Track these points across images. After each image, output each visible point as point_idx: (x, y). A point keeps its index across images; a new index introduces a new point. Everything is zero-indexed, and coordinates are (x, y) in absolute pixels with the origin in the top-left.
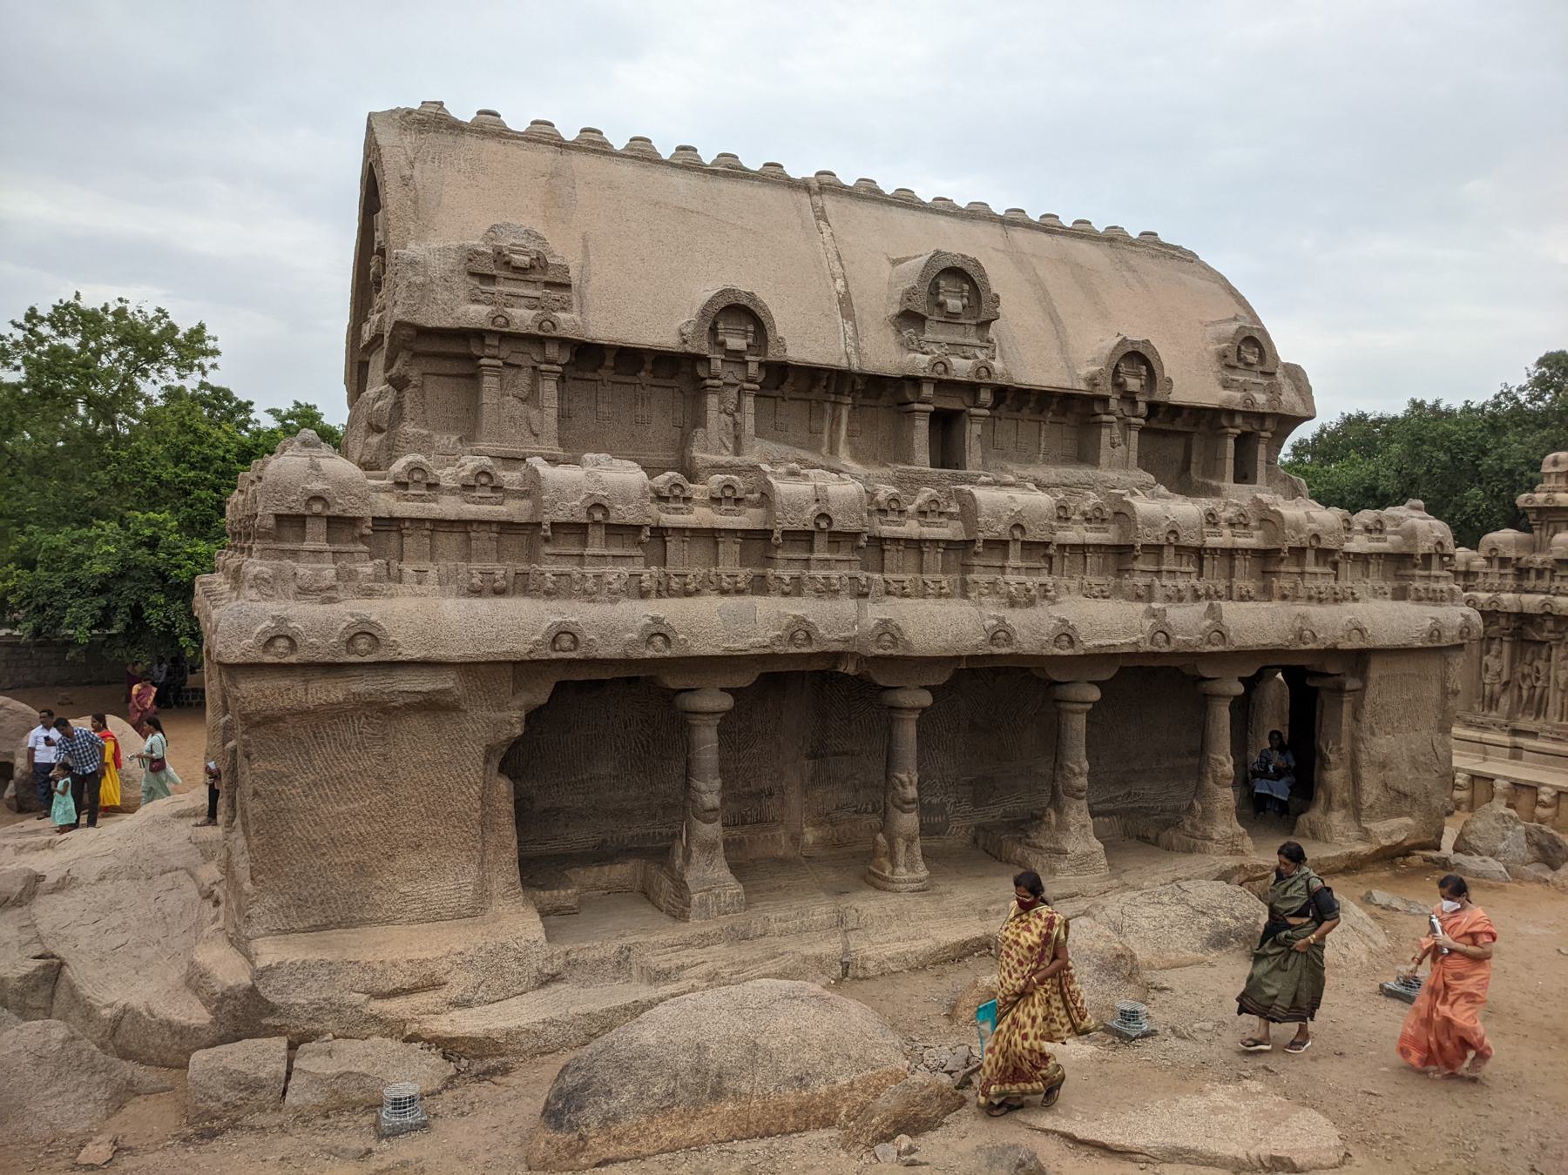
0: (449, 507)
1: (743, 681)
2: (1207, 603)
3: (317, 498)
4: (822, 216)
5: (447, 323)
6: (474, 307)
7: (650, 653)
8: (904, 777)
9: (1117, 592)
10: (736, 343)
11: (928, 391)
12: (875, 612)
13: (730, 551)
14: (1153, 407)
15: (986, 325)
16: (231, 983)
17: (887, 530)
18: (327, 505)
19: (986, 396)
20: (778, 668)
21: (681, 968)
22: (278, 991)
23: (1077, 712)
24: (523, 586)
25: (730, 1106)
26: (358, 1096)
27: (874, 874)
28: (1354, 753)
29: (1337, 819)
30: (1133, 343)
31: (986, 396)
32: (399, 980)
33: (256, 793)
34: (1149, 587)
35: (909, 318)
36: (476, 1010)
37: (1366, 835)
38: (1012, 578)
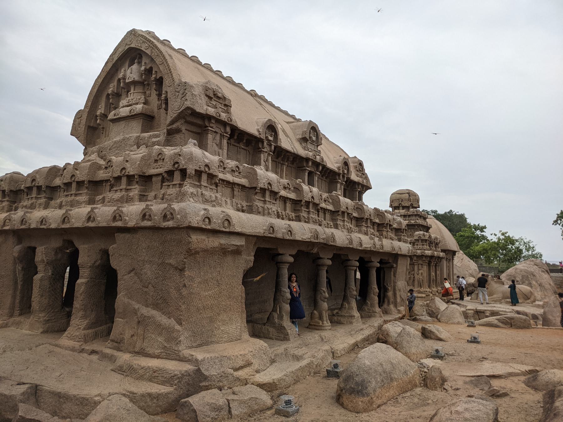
0: (229, 177)
1: (294, 252)
3: (207, 166)
6: (209, 108)
7: (288, 238)
8: (324, 289)
9: (360, 232)
10: (271, 138)
13: (288, 205)
15: (318, 146)
16: (185, 369)
18: (209, 169)
20: (303, 248)
22: (207, 370)
23: (352, 270)
24: (250, 210)
26: (256, 407)
27: (314, 325)
28: (394, 286)
29: (392, 306)
32: (241, 363)
33: (185, 286)
34: (367, 231)
35: (304, 140)
36: (262, 373)
37: (399, 312)
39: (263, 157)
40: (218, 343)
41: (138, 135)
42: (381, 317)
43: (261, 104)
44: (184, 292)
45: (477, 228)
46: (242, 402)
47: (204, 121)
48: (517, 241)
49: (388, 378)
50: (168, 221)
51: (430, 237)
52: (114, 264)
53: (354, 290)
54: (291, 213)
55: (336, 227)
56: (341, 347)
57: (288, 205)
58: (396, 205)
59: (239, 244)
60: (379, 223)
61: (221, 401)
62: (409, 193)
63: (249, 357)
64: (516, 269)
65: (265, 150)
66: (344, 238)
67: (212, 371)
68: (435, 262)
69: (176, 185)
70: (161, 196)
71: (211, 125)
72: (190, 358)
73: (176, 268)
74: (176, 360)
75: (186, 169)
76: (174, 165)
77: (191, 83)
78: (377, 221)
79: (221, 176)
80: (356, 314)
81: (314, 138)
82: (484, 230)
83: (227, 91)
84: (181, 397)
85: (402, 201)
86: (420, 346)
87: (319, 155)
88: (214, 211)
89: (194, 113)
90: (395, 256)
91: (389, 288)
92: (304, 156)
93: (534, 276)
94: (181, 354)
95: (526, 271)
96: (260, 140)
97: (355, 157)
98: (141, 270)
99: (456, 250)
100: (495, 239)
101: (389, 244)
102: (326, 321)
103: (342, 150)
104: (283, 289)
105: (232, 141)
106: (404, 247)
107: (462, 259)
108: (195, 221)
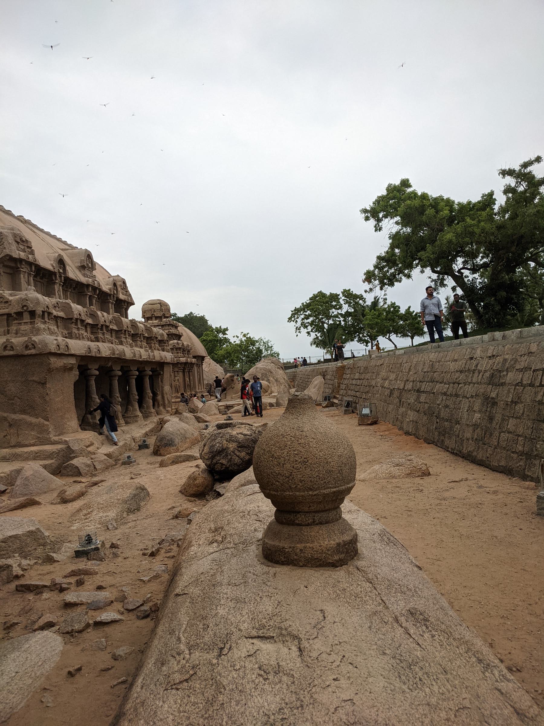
4: (34, 232)
5: (17, 257)
9: (136, 346)
10: (61, 271)
14: (117, 298)
24: (70, 336)
28: (162, 390)
31: (98, 292)
32: (89, 443)
33: (47, 394)
35: (82, 268)
39: (56, 287)
40: (67, 433)
42: (156, 416)
43: (34, 232)
44: (47, 398)
45: (219, 330)
47: (16, 263)
48: (257, 341)
49: (184, 438)
50: (30, 349)
51: (183, 345)
53: (135, 396)
54: (91, 336)
55: (121, 343)
56: (138, 435)
57: (89, 329)
58: (149, 316)
59: (73, 363)
60: (134, 334)
61: (89, 462)
62: (160, 303)
63: (91, 439)
64: (257, 368)
65: (57, 281)
66: (130, 352)
67: (75, 447)
68: (188, 367)
69: (27, 322)
70: (14, 332)
71: (23, 266)
72: (60, 441)
73: (39, 383)
74: (49, 444)
75: (34, 311)
76: (23, 307)
78: (146, 335)
80: (139, 413)
81: (90, 265)
82: (226, 332)
83: (27, 234)
85: (154, 311)
89: (11, 258)
90: (162, 364)
92: (85, 283)
93: (271, 372)
94: (52, 440)
95: (265, 369)
96: (54, 274)
97: (118, 276)
98: (4, 388)
99: (205, 355)
100: (238, 342)
101: (159, 355)
103: (106, 270)
104: (93, 396)
106: (168, 356)
107: (209, 364)
108: (53, 348)
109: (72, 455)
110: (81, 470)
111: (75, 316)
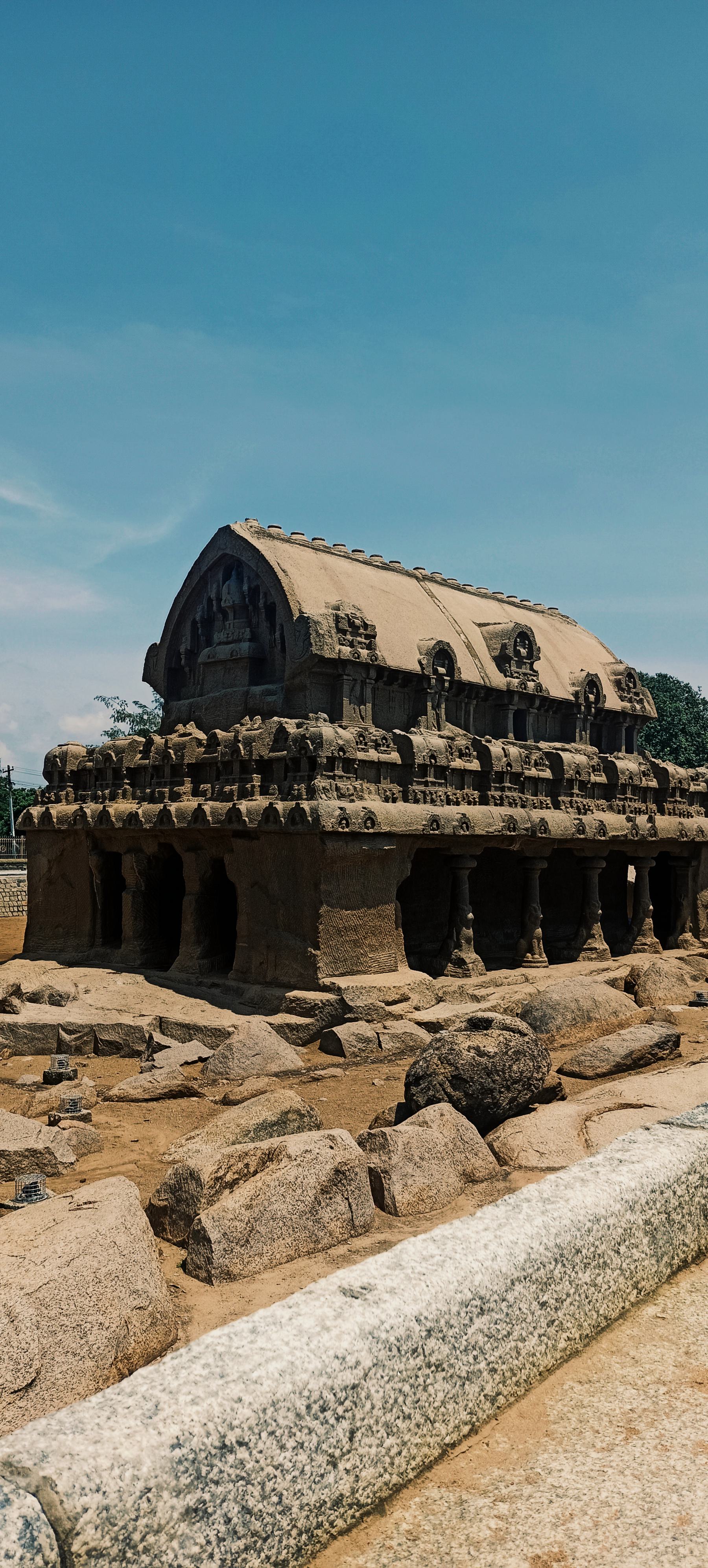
0: (373, 755)
2: (647, 817)
3: (341, 749)
4: (432, 596)
5: (334, 656)
6: (343, 648)
10: (442, 670)
11: (516, 698)
12: (536, 814)
15: (532, 664)
17: (527, 773)
19: (537, 703)
21: (488, 995)
25: (595, 1024)
30: (592, 675)
38: (579, 799)
41: (245, 689)
46: (394, 1036)
52: (232, 876)
55: (557, 806)
61: (370, 1034)
63: (405, 990)
77: (315, 618)
79: (361, 755)
84: (323, 1028)
86: (675, 989)
87: (533, 681)
88: (353, 807)
91: (685, 903)
94: (321, 982)
102: (540, 955)
105: (380, 684)
109: (349, 1015)
110: (346, 1046)
111: (419, 761)
